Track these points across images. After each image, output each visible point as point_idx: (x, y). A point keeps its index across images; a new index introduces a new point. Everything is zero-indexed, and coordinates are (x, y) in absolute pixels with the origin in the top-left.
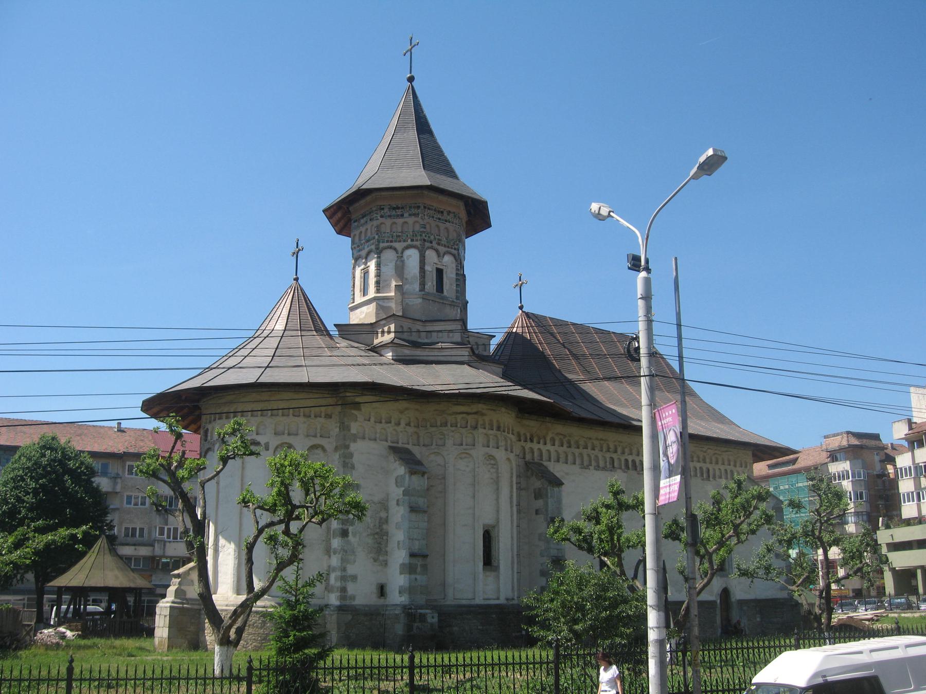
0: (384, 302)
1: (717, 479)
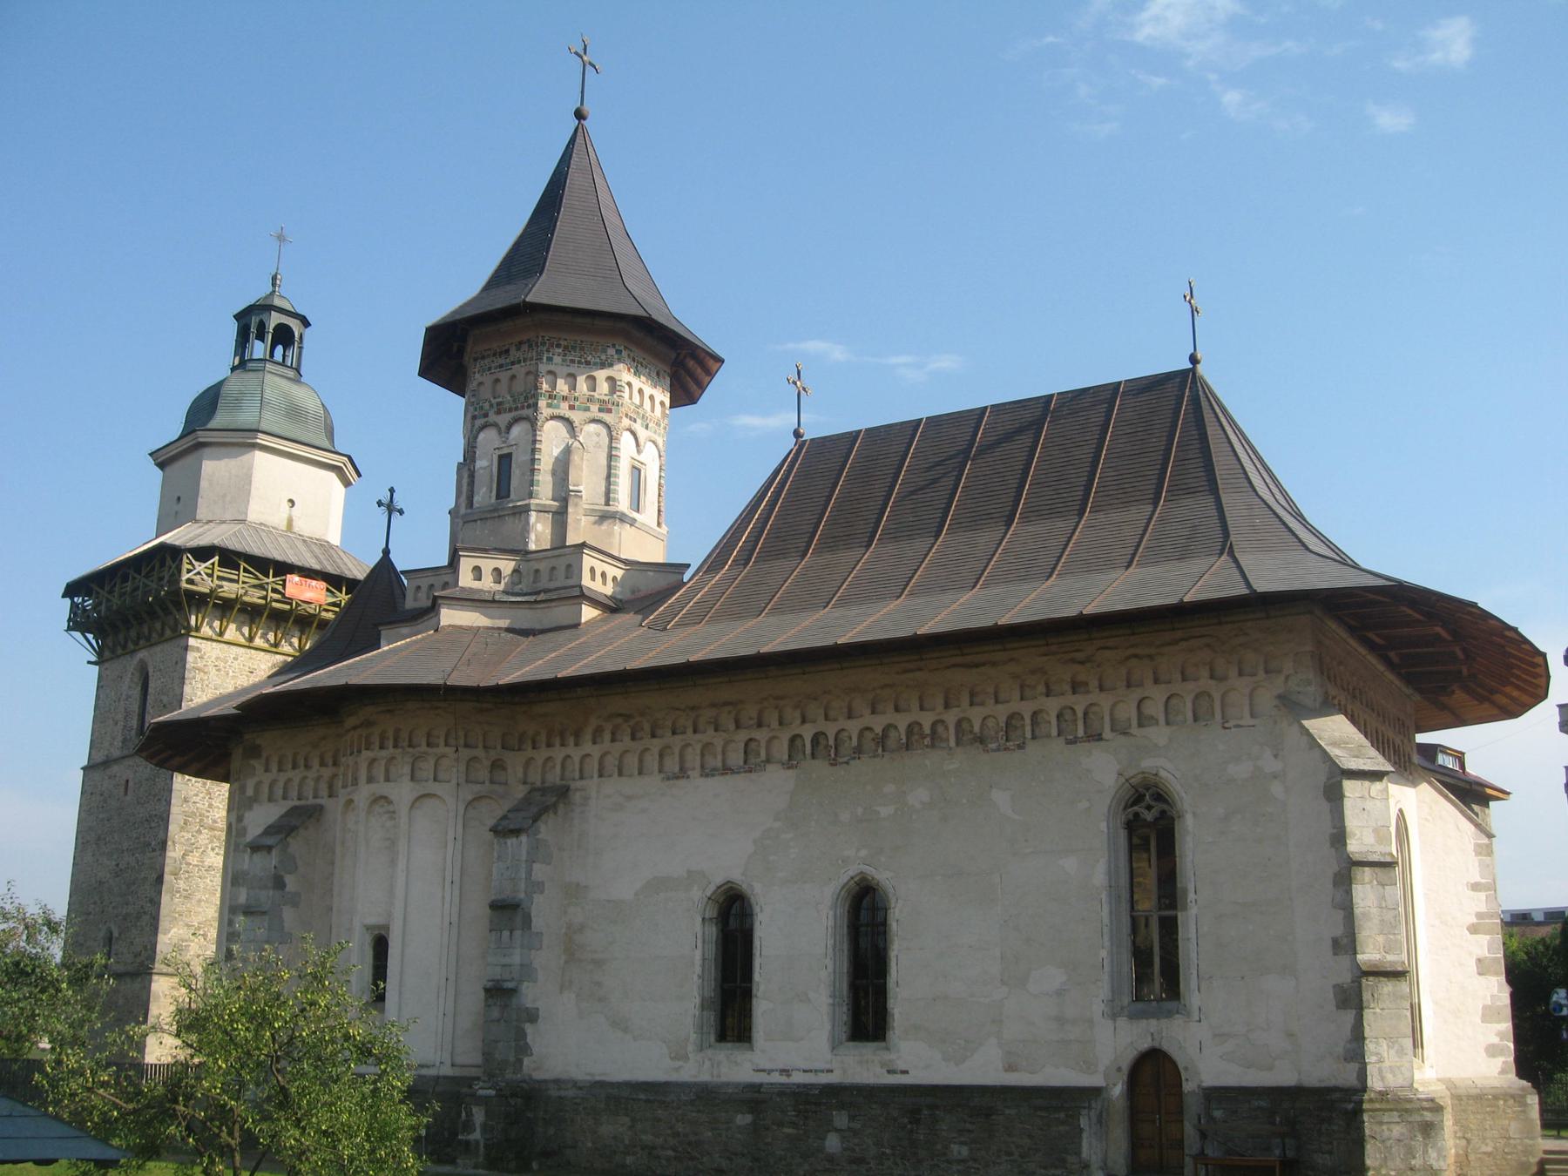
1: (1134, 730)
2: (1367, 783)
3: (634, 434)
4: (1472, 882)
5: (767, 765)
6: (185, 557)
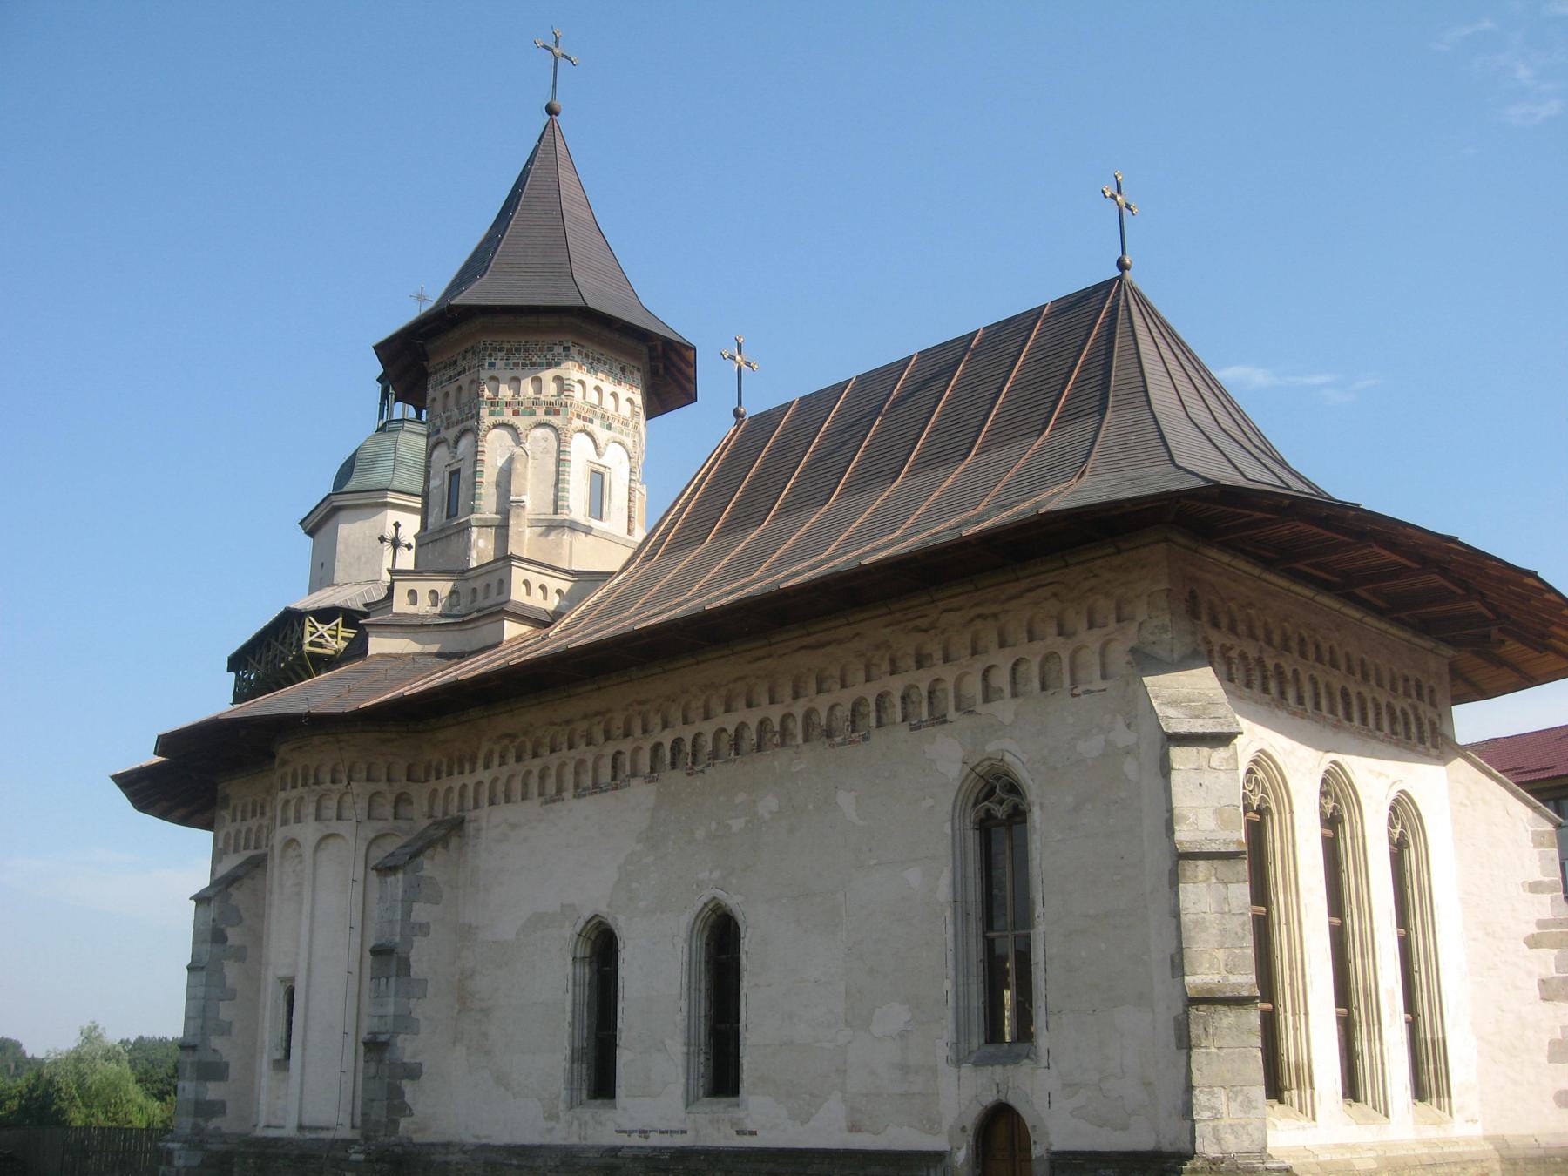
1: (980, 708)
2: (1205, 751)
3: (590, 435)
4: (1531, 881)
5: (631, 780)
6: (307, 620)
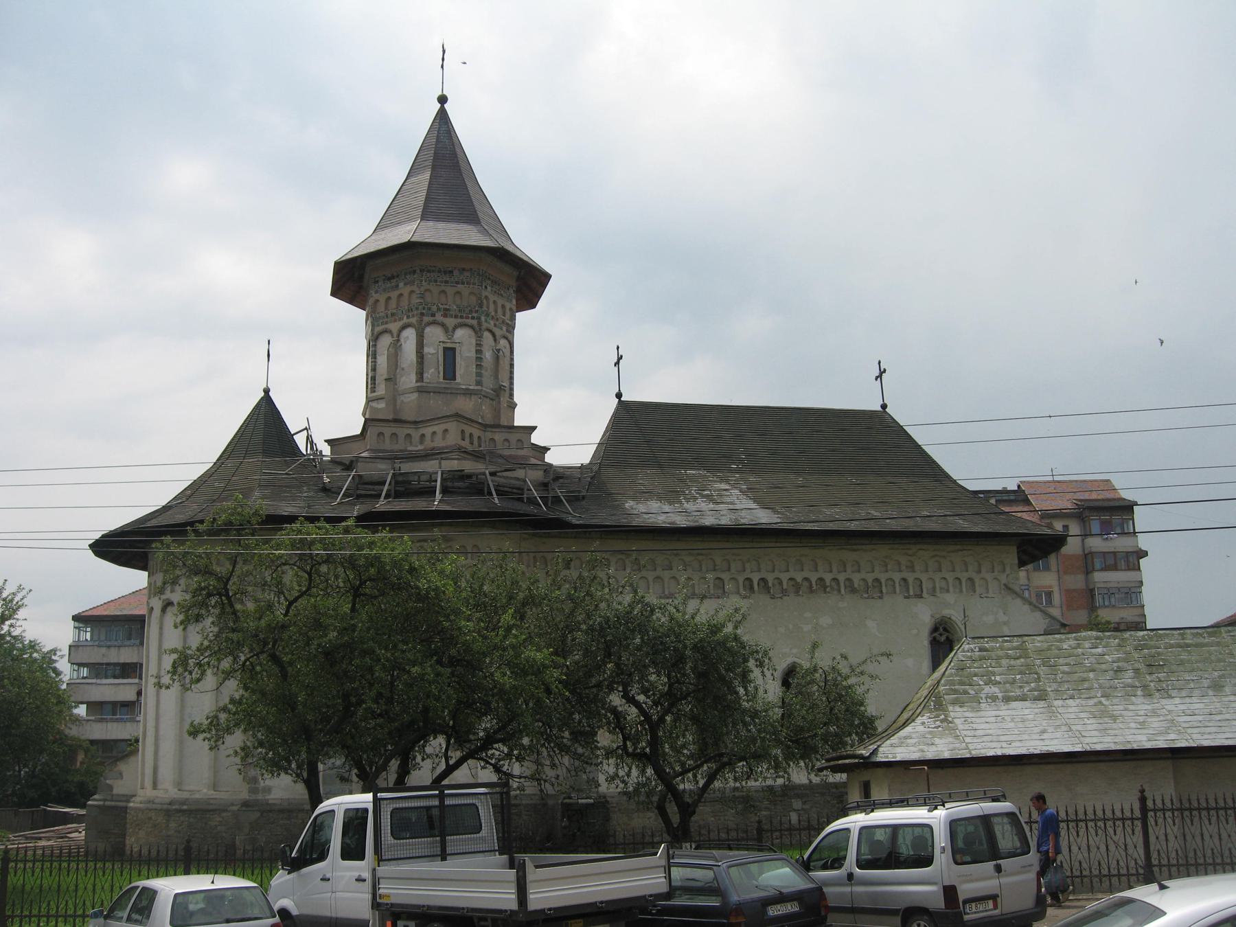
0: (378, 403)
1: (938, 594)
